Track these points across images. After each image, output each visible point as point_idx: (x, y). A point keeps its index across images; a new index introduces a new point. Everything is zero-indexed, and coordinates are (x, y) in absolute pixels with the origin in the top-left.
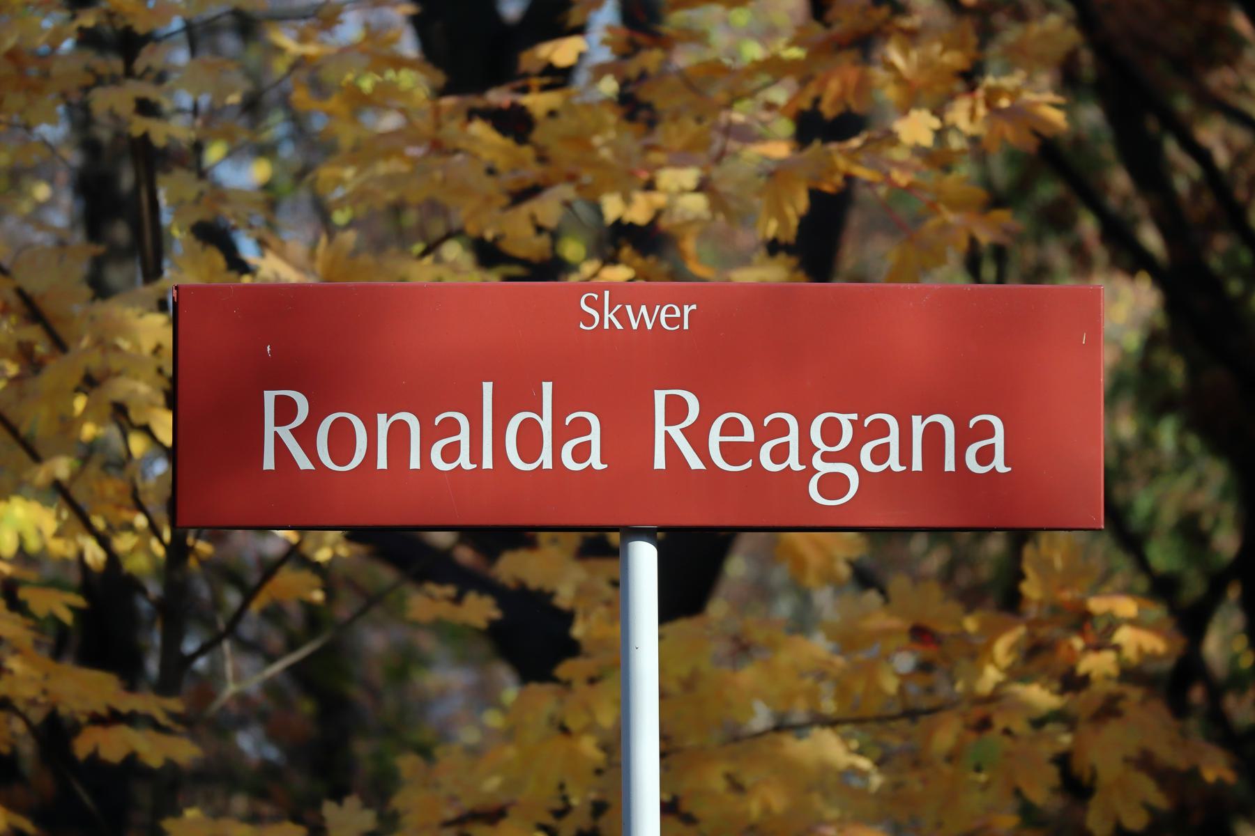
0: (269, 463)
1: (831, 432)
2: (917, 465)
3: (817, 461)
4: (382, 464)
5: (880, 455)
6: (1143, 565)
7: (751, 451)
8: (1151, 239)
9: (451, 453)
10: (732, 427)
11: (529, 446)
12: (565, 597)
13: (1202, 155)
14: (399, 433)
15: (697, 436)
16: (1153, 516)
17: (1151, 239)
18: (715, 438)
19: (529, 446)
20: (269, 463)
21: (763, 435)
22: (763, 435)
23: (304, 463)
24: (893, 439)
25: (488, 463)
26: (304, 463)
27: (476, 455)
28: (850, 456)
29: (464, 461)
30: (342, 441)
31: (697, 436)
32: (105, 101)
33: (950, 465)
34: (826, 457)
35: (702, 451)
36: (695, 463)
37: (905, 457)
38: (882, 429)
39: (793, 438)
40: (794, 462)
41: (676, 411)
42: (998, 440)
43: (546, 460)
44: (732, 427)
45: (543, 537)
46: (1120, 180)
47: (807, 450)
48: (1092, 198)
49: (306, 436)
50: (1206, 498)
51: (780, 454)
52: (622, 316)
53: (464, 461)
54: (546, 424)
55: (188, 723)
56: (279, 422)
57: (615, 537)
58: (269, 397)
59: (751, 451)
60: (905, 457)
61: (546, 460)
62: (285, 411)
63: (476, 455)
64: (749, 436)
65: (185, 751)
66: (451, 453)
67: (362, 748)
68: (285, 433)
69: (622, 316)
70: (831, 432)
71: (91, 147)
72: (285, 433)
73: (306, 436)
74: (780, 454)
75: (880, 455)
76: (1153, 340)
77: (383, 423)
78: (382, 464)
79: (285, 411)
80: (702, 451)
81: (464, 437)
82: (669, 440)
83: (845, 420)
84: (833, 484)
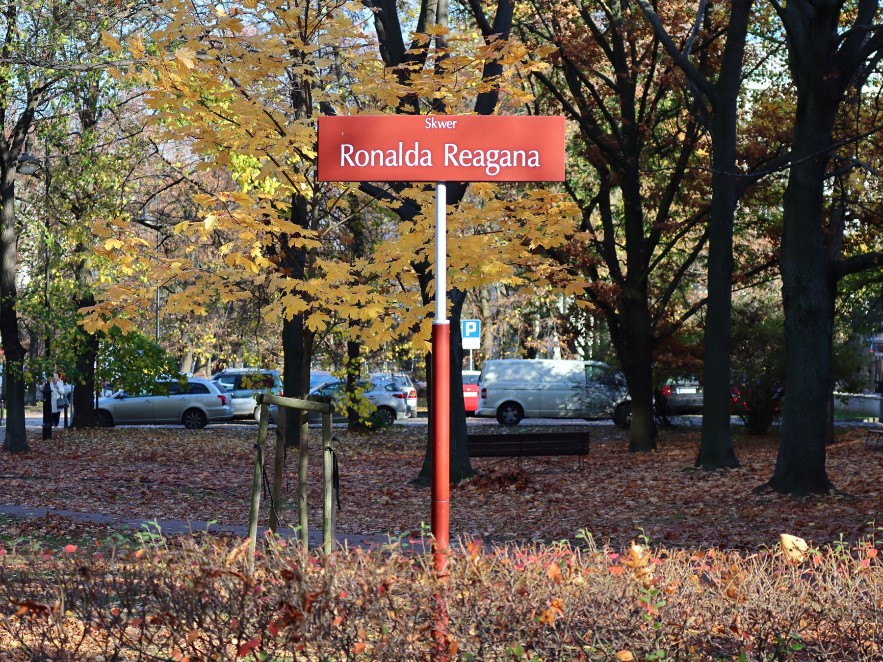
0: (343, 164)
1: (492, 156)
2: (515, 164)
3: (488, 163)
4: (373, 164)
5: (505, 162)
6: (575, 199)
7: (471, 161)
8: (577, 110)
9: (391, 161)
10: (466, 154)
11: (412, 159)
12: (419, 202)
13: (591, 87)
14: (377, 155)
15: (457, 157)
16: (577, 183)
17: (577, 110)
18: (461, 157)
19: (412, 159)
20: (343, 164)
21: (474, 156)
22: (474, 156)
23: (352, 164)
24: (509, 157)
25: (401, 164)
26: (352, 164)
27: (398, 162)
28: (497, 162)
29: (394, 163)
30: (362, 158)
31: (457, 157)
32: (299, 70)
33: (524, 164)
34: (491, 162)
35: (458, 160)
36: (456, 164)
37: (512, 162)
38: (505, 154)
39: (482, 157)
40: (482, 164)
41: (451, 150)
42: (537, 158)
43: (416, 163)
44: (466, 154)
45: (414, 184)
46: (568, 93)
47: (486, 160)
48: (560, 97)
49: (352, 157)
50: (591, 179)
51: (478, 161)
52: (437, 124)
53: (394, 163)
54: (416, 153)
55: (318, 238)
56: (346, 153)
57: (433, 185)
58: (343, 146)
59: (471, 161)
60: (512, 162)
61: (416, 163)
62: (347, 150)
63: (398, 162)
64: (470, 156)
65: (317, 244)
66: (391, 161)
67: (367, 247)
68: (347, 156)
69: (437, 124)
70: (492, 156)
71: (295, 84)
72: (347, 156)
73: (352, 157)
74: (478, 161)
75: (505, 162)
76: (576, 136)
77: (373, 153)
78: (373, 164)
79: (347, 150)
80: (458, 160)
81: (394, 157)
82: (449, 158)
83: (496, 152)
84: (493, 170)
